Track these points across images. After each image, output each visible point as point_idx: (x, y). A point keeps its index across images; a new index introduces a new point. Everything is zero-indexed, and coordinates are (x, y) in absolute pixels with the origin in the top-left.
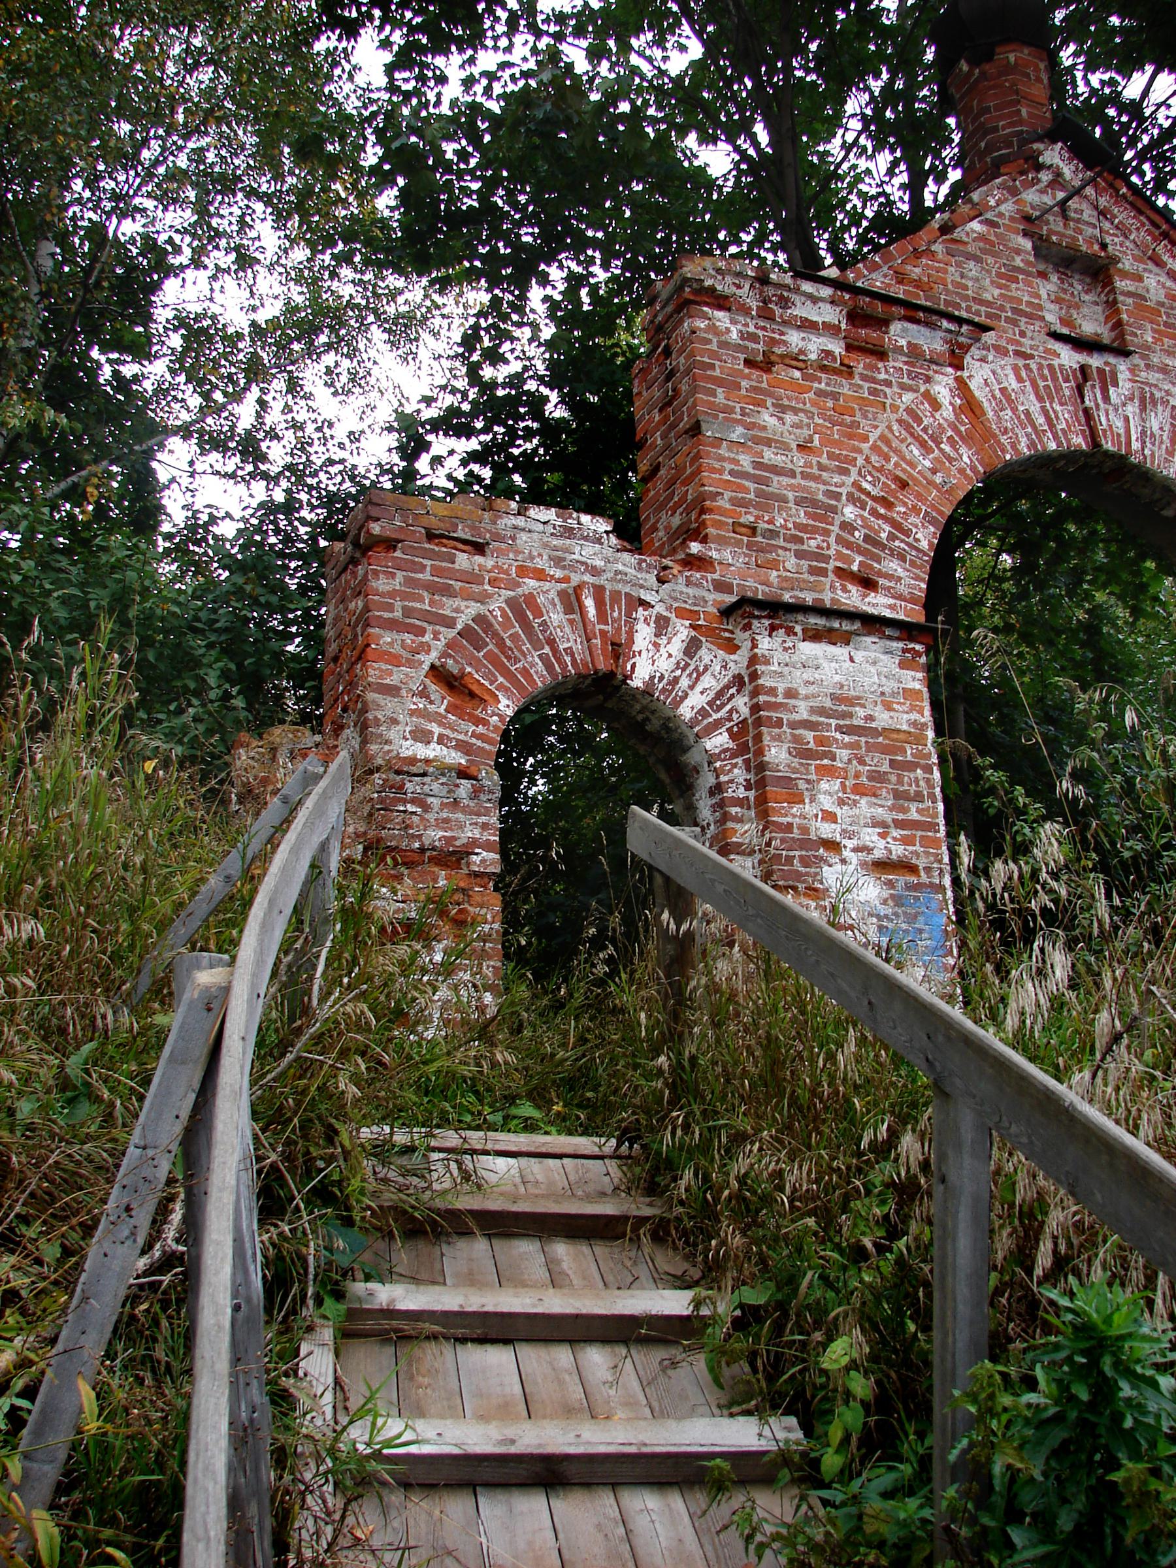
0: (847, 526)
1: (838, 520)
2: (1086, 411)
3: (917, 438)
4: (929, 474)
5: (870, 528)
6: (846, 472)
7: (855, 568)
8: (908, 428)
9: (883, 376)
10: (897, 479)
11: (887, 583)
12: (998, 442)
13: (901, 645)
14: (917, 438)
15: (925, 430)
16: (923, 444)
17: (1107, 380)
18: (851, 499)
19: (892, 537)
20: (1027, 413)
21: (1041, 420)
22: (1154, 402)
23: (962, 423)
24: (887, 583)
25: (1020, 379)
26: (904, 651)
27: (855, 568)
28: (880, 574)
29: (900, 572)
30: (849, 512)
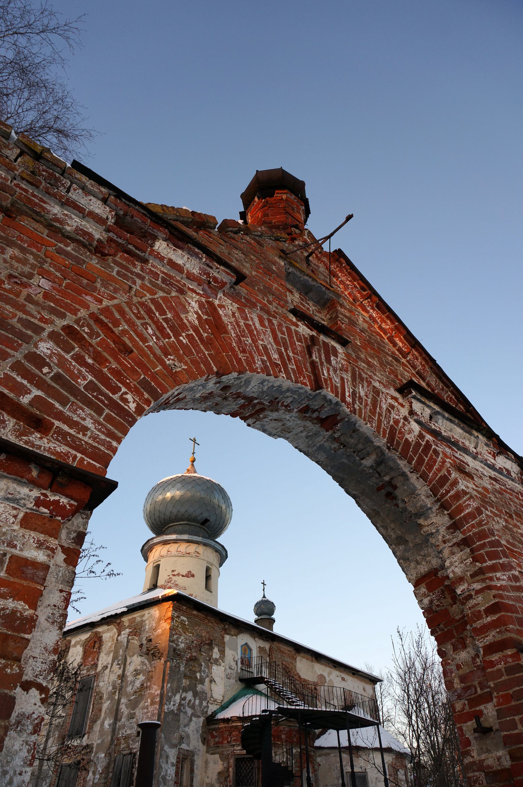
0: (39, 361)
1: (25, 348)
2: (313, 364)
3: (157, 323)
4: (158, 352)
5: (68, 370)
6: (63, 316)
7: (25, 400)
8: (149, 312)
9: (138, 270)
10: (118, 340)
11: (65, 428)
12: (236, 356)
13: (36, 493)
14: (157, 323)
15: (166, 320)
16: (160, 329)
17: (330, 352)
18: (53, 336)
19: (90, 386)
20: (265, 347)
21: (276, 356)
22: (362, 379)
23: (205, 331)
24: (65, 428)
25: (262, 324)
26: (38, 502)
27: (25, 400)
28: (60, 416)
29: (89, 423)
30: (45, 348)
